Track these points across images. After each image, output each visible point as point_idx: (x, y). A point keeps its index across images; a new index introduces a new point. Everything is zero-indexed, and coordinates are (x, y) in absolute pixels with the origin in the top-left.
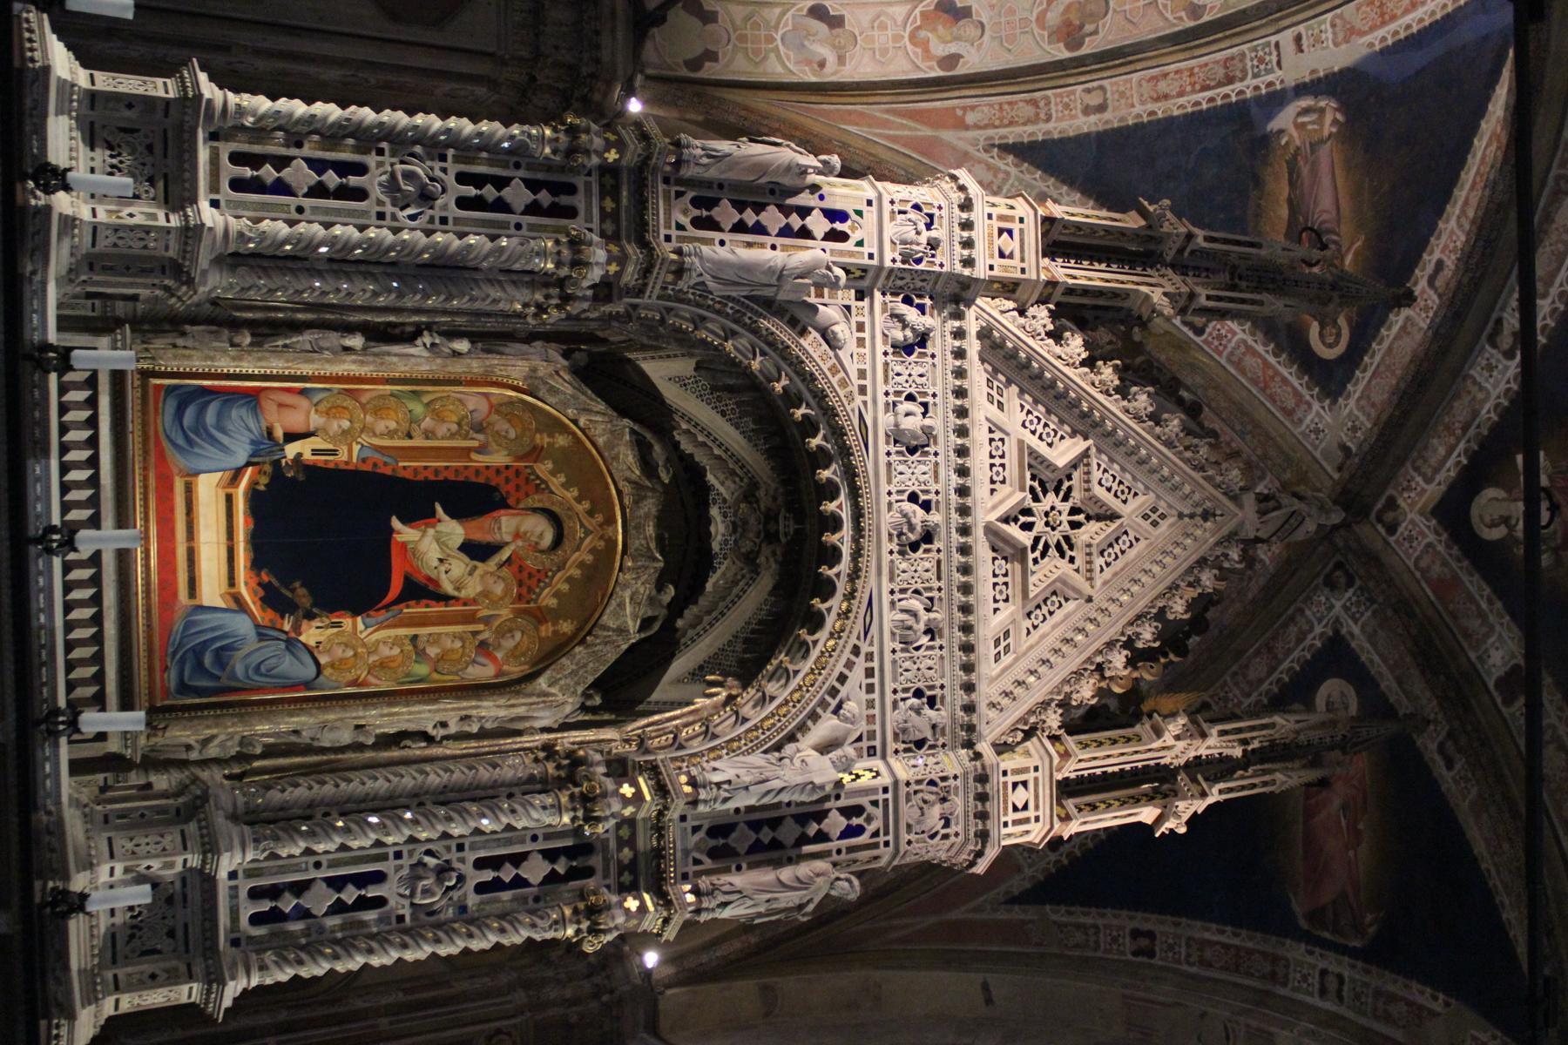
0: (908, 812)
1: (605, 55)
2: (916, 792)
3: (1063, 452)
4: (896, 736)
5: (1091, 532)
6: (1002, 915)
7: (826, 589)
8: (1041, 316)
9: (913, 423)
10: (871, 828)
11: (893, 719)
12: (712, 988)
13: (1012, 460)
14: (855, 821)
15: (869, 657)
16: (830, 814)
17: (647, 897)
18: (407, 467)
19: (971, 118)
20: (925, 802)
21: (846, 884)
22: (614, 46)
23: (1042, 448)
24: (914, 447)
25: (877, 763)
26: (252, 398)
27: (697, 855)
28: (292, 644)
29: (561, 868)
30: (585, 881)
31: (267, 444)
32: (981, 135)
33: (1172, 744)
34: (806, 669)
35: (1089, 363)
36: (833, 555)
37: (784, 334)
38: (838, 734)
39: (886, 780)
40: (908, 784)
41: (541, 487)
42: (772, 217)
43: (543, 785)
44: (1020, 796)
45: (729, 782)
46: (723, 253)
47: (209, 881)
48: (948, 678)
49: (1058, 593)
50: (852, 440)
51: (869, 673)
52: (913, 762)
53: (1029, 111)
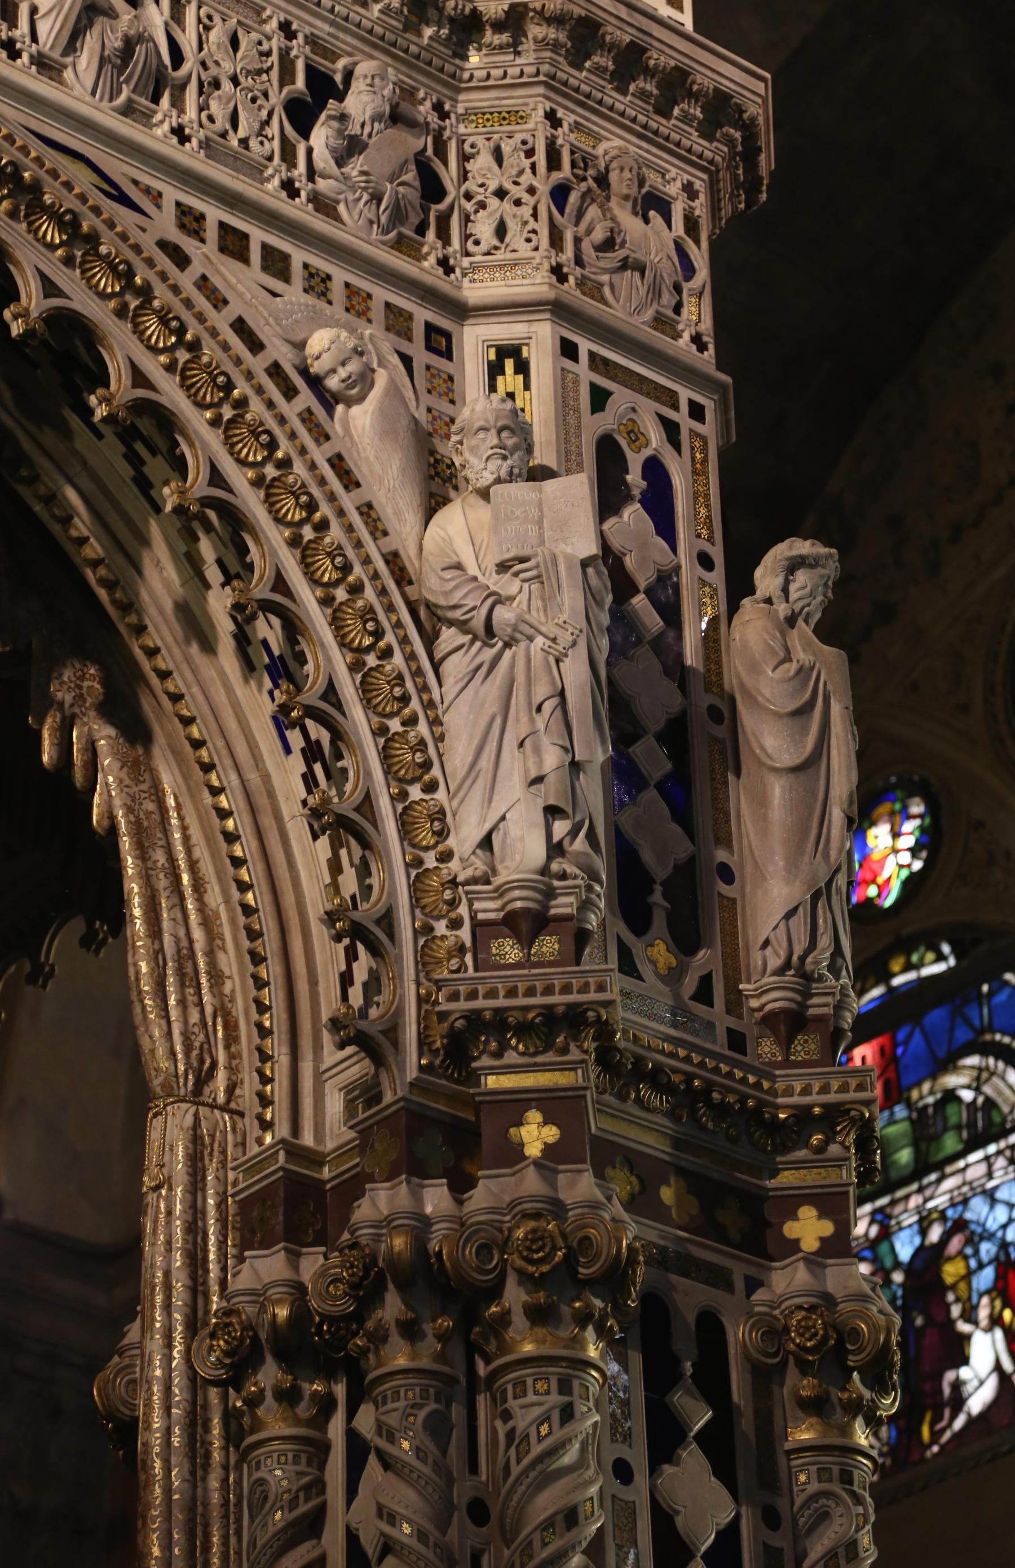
2: (579, 262)
4: (400, 245)
10: (656, 437)
14: (634, 477)
15: (190, 221)
16: (616, 543)
17: (787, 1178)
20: (608, 245)
21: (801, 577)
25: (475, 341)
27: (690, 984)
29: (702, 1418)
30: (733, 1351)
34: (213, 439)
38: (404, 422)
39: (540, 337)
40: (558, 272)
45: (552, 812)
51: (233, 244)
52: (484, 228)
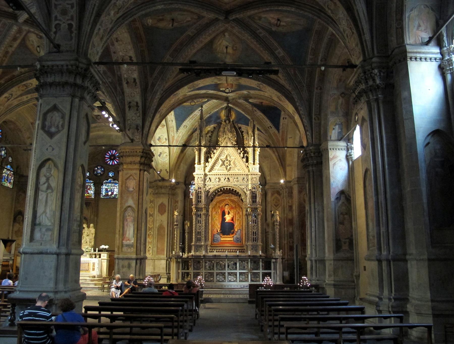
0: (254, 182)
1: (168, 185)
3: (220, 162)
5: (228, 158)
6: (281, 134)
7: (233, 190)
8: (207, 164)
9: (217, 180)
11: (245, 183)
12: (288, 173)
13: (221, 168)
18: (220, 220)
19: (173, 135)
22: (167, 184)
23: (220, 164)
24: (220, 179)
26: (214, 235)
28: (237, 232)
31: (218, 234)
32: (175, 134)
33: (250, 150)
35: (211, 158)
36: (230, 189)
37: (210, 194)
41: (222, 206)
42: (200, 195)
43: (248, 218)
44: (254, 169)
46: (203, 201)
47: (252, 245)
48: (242, 176)
49: (234, 163)
50: (219, 186)
53: (172, 128)
